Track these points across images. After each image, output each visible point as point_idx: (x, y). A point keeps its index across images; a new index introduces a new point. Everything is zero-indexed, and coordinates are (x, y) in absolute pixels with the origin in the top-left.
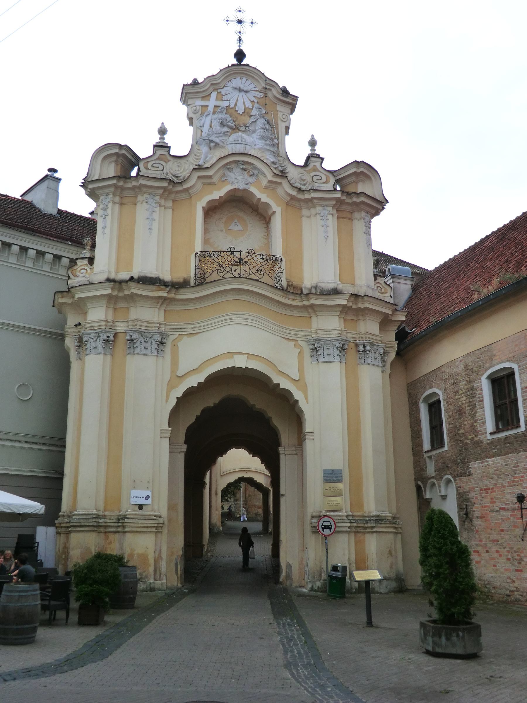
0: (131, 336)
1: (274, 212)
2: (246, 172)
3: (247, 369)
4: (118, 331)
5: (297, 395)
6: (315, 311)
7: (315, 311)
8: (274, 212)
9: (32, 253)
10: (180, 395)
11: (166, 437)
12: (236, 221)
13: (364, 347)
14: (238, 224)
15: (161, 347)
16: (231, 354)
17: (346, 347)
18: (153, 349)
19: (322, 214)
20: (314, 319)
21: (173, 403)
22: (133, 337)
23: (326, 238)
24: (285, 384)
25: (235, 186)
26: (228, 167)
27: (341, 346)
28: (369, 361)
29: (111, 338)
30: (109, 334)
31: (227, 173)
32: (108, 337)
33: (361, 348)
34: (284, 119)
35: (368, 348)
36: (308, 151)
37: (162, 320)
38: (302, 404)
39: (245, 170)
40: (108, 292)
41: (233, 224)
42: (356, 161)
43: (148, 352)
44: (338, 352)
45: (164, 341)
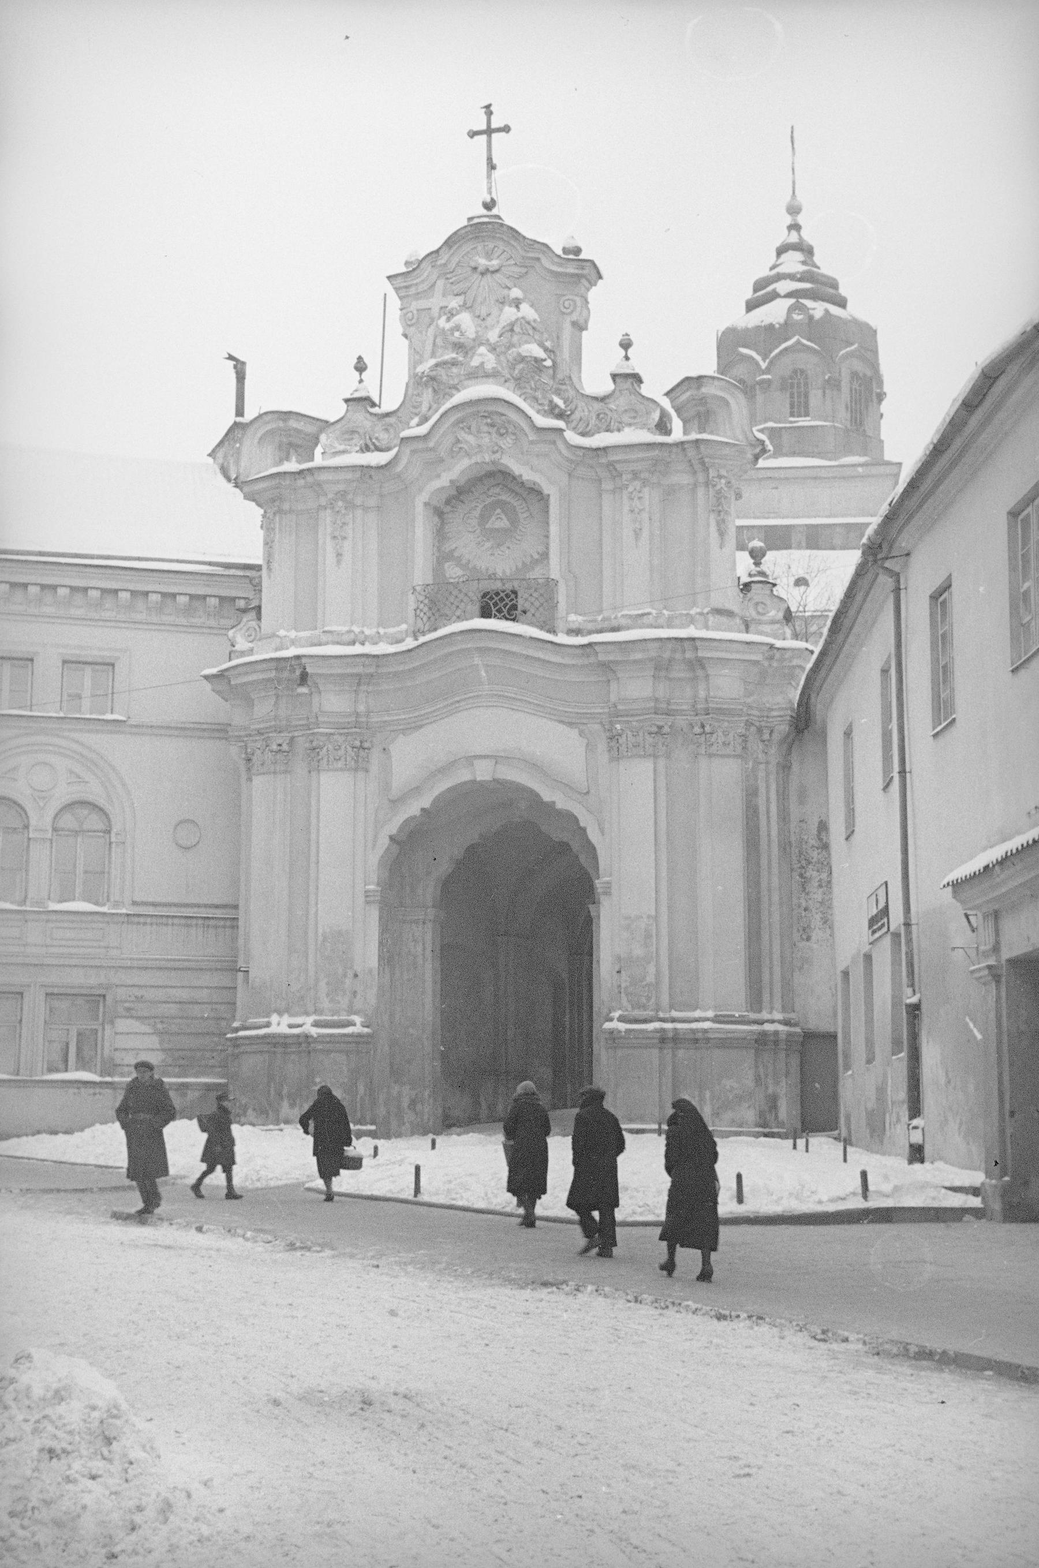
0: (312, 742)
1: (549, 495)
2: (496, 428)
3: (495, 780)
4: (296, 734)
5: (585, 820)
6: (614, 672)
7: (614, 672)
8: (549, 495)
9: (182, 600)
10: (394, 831)
11: (373, 902)
12: (498, 511)
13: (703, 726)
14: (503, 517)
15: (362, 753)
16: (470, 760)
17: (666, 729)
18: (348, 759)
19: (630, 489)
20: (614, 686)
21: (384, 842)
22: (315, 744)
23: (637, 533)
24: (562, 803)
25: (478, 459)
26: (461, 425)
27: (655, 729)
28: (713, 749)
29: (285, 747)
30: (280, 742)
31: (463, 435)
32: (280, 745)
33: (697, 730)
34: (565, 307)
35: (708, 729)
36: (615, 361)
37: (361, 708)
38: (593, 835)
39: (492, 425)
40: (273, 674)
41: (493, 518)
42: (687, 379)
43: (340, 764)
44: (651, 740)
45: (366, 745)
